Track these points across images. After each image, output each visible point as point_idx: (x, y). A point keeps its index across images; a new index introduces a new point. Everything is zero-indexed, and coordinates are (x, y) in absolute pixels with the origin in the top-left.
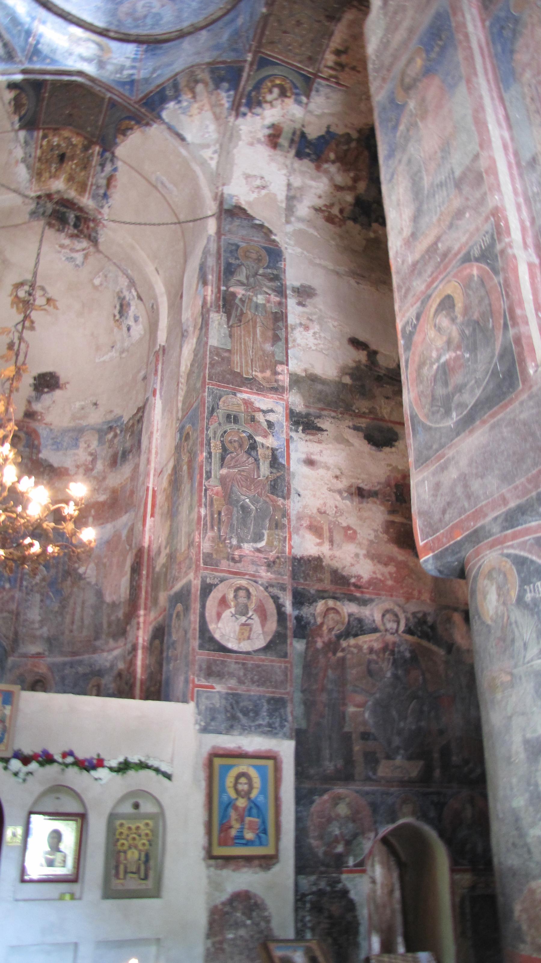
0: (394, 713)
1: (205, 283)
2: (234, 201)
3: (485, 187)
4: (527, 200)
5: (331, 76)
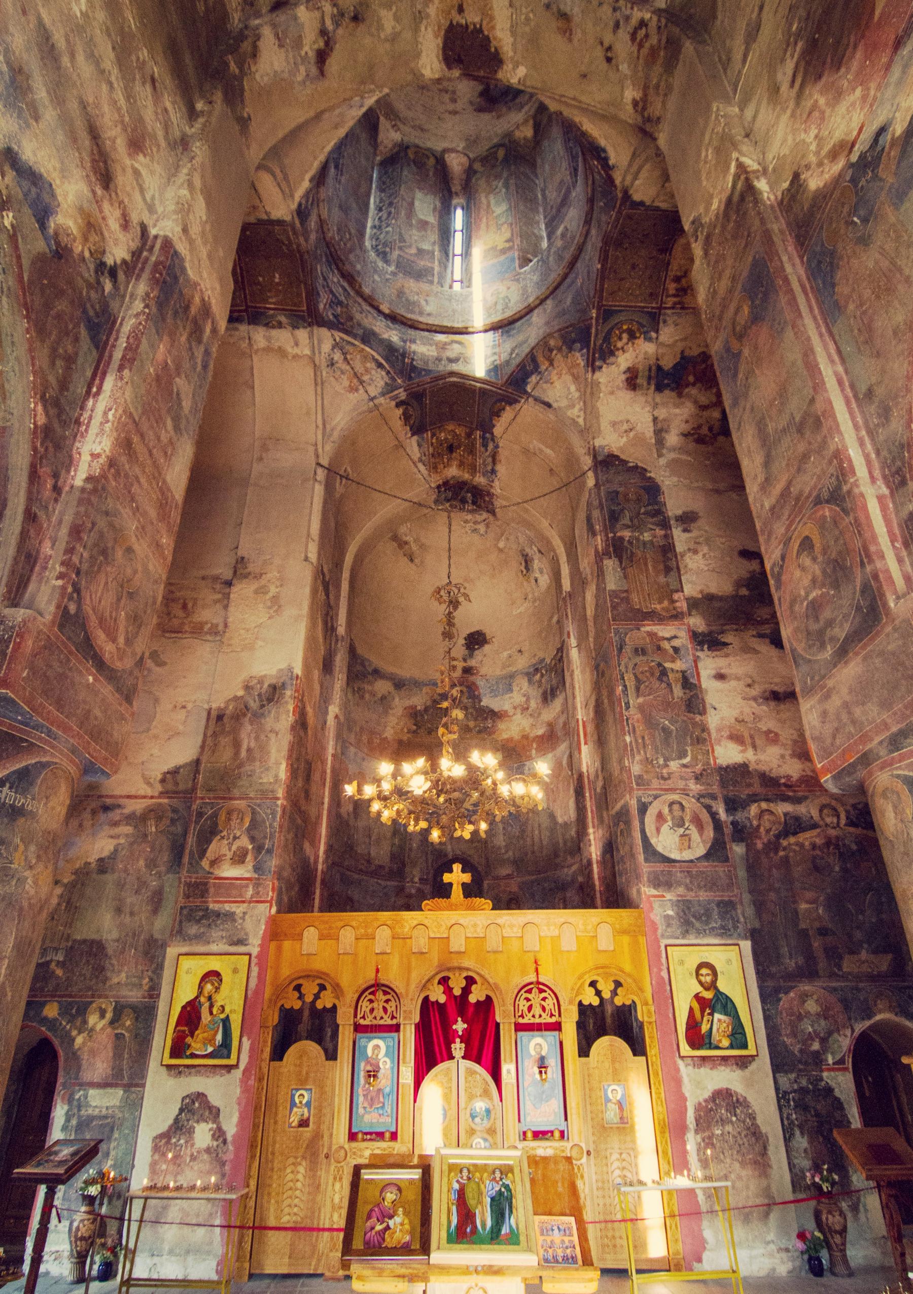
1: (594, 534)
3: (825, 431)
4: (870, 432)
5: (675, 303)
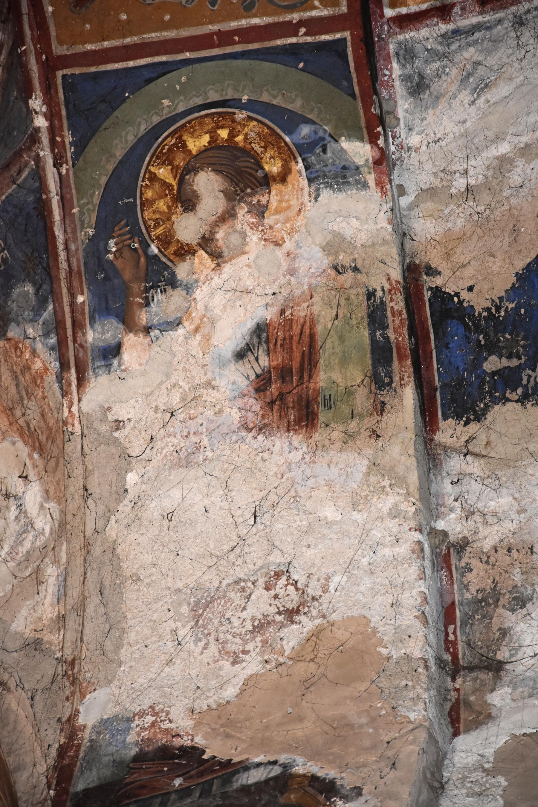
2: (133, 739)
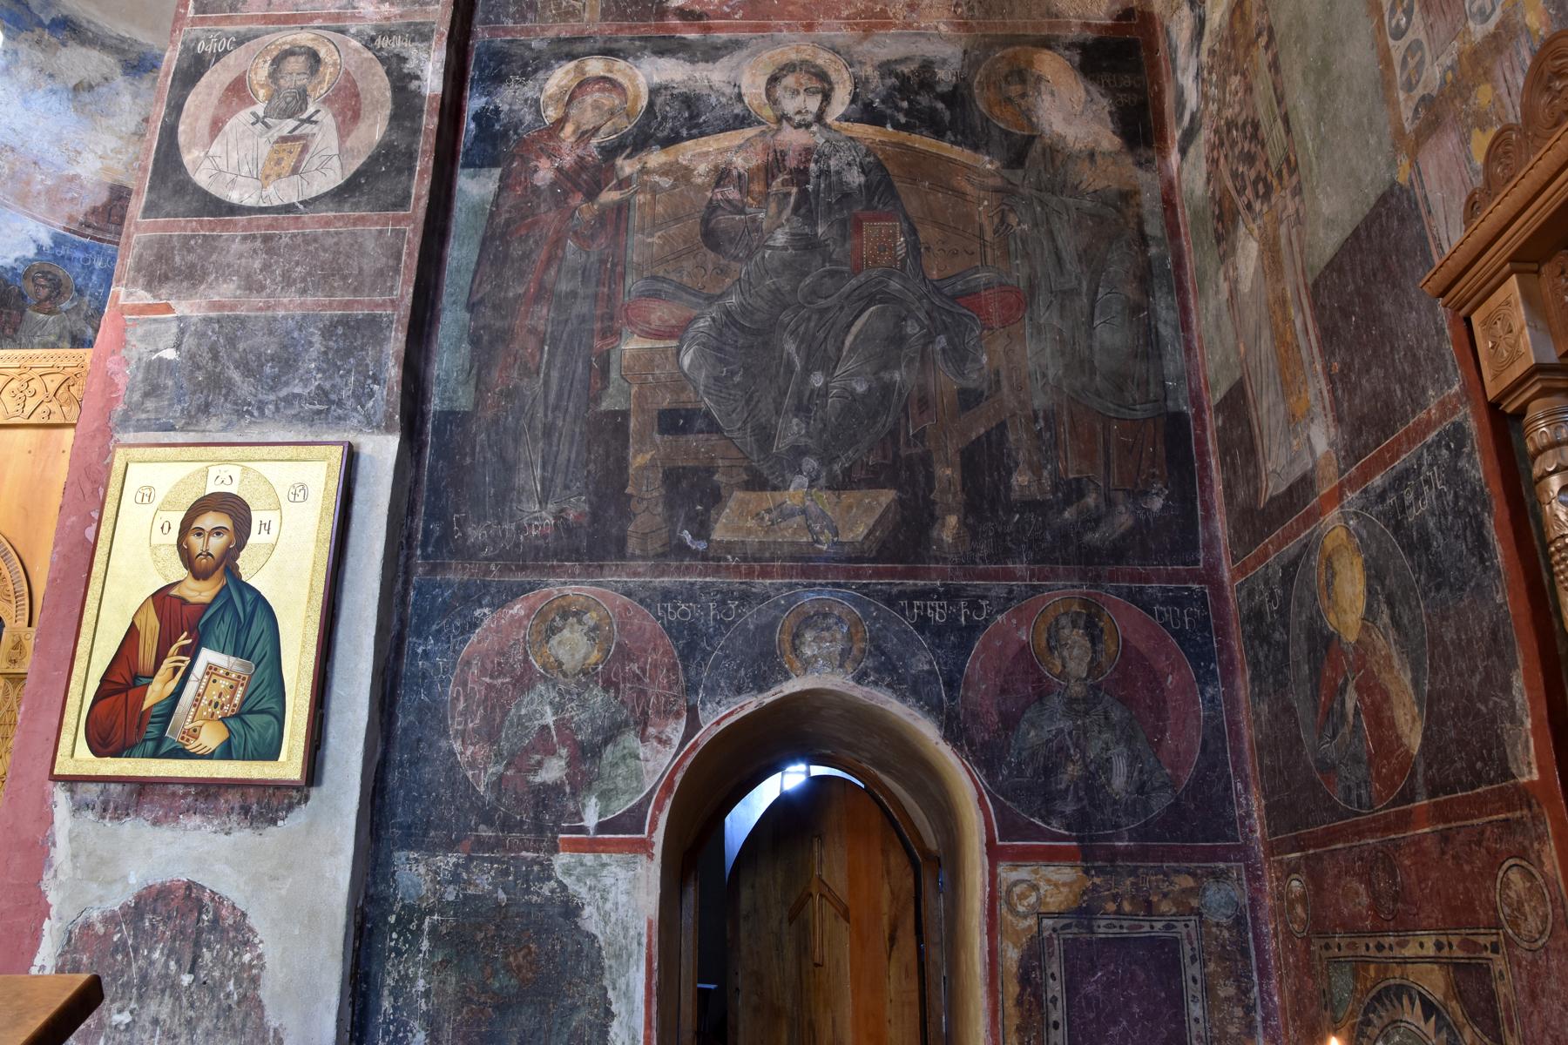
0: (790, 347)
